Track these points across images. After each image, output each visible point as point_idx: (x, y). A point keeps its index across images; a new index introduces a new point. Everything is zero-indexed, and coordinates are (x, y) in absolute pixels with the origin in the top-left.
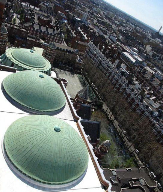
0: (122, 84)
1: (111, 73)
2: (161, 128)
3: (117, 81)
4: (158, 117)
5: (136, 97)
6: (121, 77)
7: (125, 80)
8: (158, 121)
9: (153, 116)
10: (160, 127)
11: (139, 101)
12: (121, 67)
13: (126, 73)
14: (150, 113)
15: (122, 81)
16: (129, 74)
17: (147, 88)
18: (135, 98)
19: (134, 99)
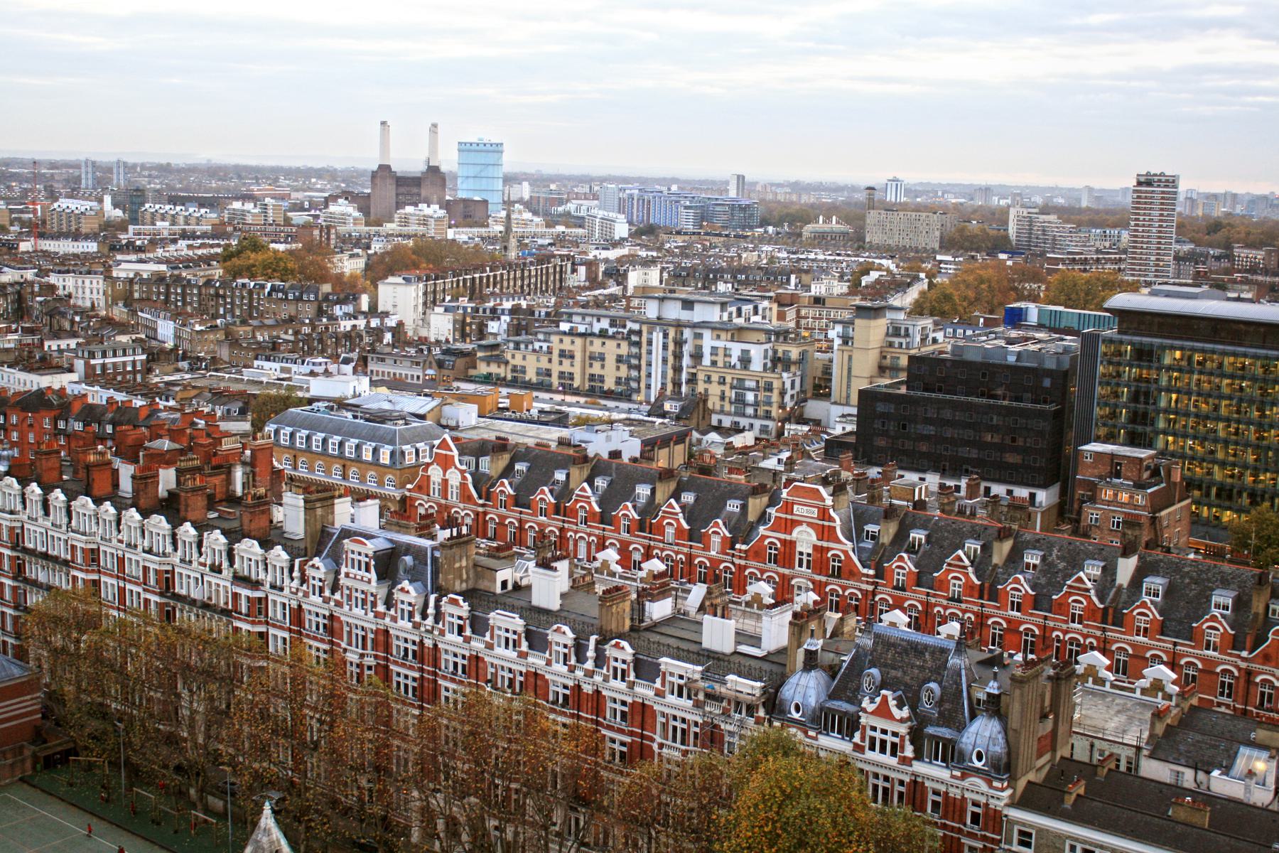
0: (428, 643)
1: (297, 615)
2: (905, 761)
3: (383, 639)
4: (832, 696)
5: (589, 665)
6: (389, 603)
7: (438, 601)
8: (849, 726)
9: (796, 716)
10: (894, 754)
11: (632, 677)
12: (346, 533)
13: (408, 549)
14: (761, 713)
15: (416, 626)
16: (434, 549)
17: (605, 564)
18: (589, 674)
19: (588, 689)
